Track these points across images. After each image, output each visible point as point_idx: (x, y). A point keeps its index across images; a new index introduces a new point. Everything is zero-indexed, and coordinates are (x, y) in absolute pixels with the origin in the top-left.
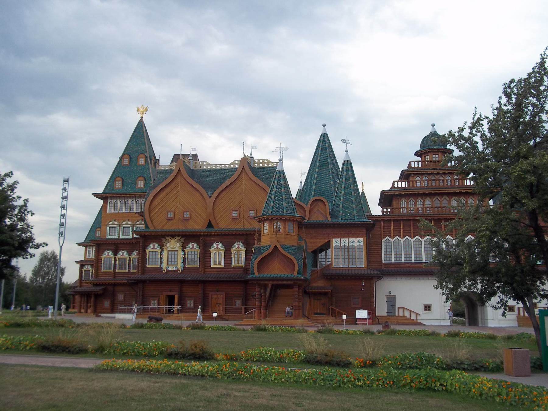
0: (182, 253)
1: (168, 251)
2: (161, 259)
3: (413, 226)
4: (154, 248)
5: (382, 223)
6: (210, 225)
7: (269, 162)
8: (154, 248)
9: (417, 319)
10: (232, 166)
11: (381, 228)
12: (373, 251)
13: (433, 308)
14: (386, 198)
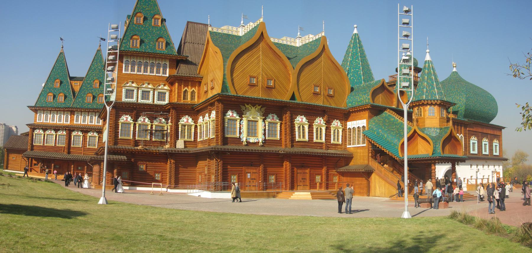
2: (240, 129)
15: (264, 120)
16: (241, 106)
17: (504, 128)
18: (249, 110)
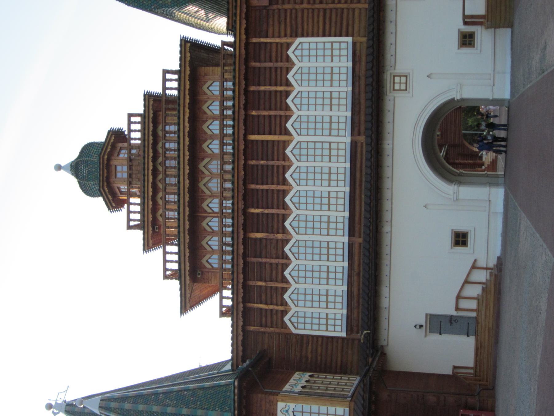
3: (261, 257)
5: (252, 328)
9: (487, 269)
11: (264, 333)
13: (461, 228)
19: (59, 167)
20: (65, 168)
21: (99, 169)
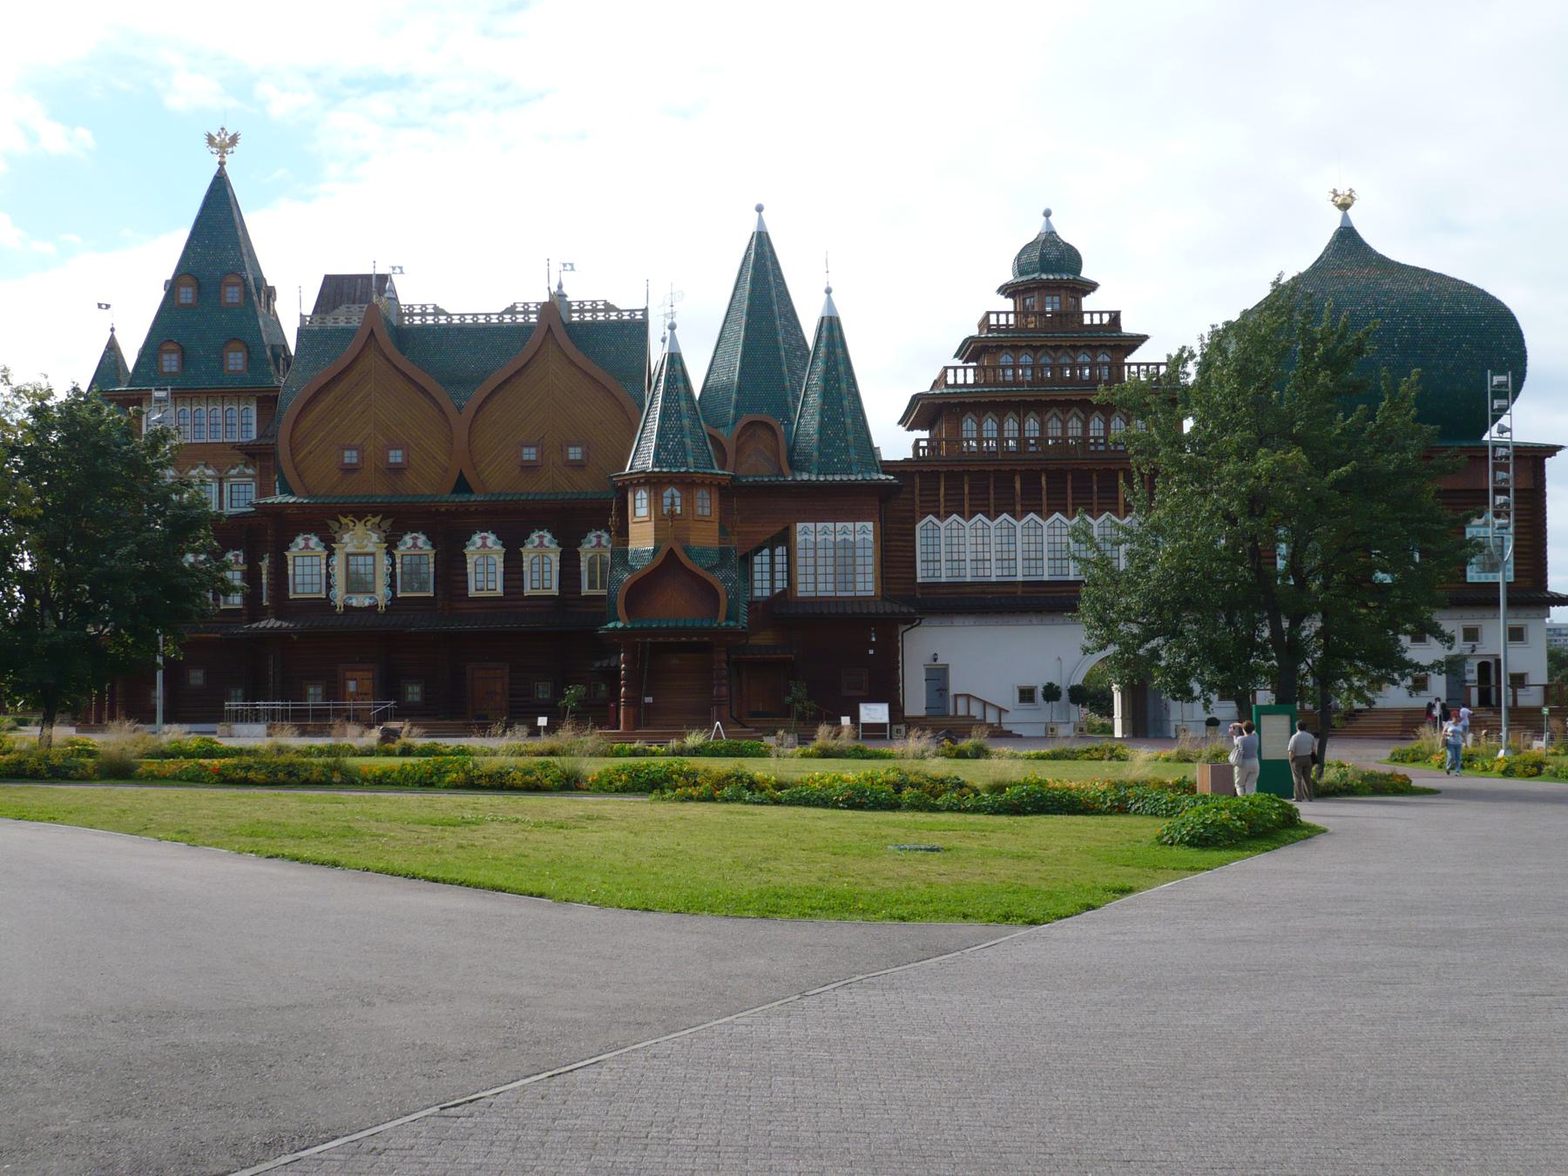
0: (386, 561)
1: (348, 555)
2: (329, 576)
4: (307, 547)
6: (462, 486)
7: (609, 308)
8: (307, 547)
10: (507, 319)
11: (912, 493)
12: (896, 553)
14: (923, 411)
15: (390, 554)
16: (331, 522)
17: (1552, 450)
18: (348, 530)
19: (1047, 214)
20: (1048, 223)
21: (1050, 273)
